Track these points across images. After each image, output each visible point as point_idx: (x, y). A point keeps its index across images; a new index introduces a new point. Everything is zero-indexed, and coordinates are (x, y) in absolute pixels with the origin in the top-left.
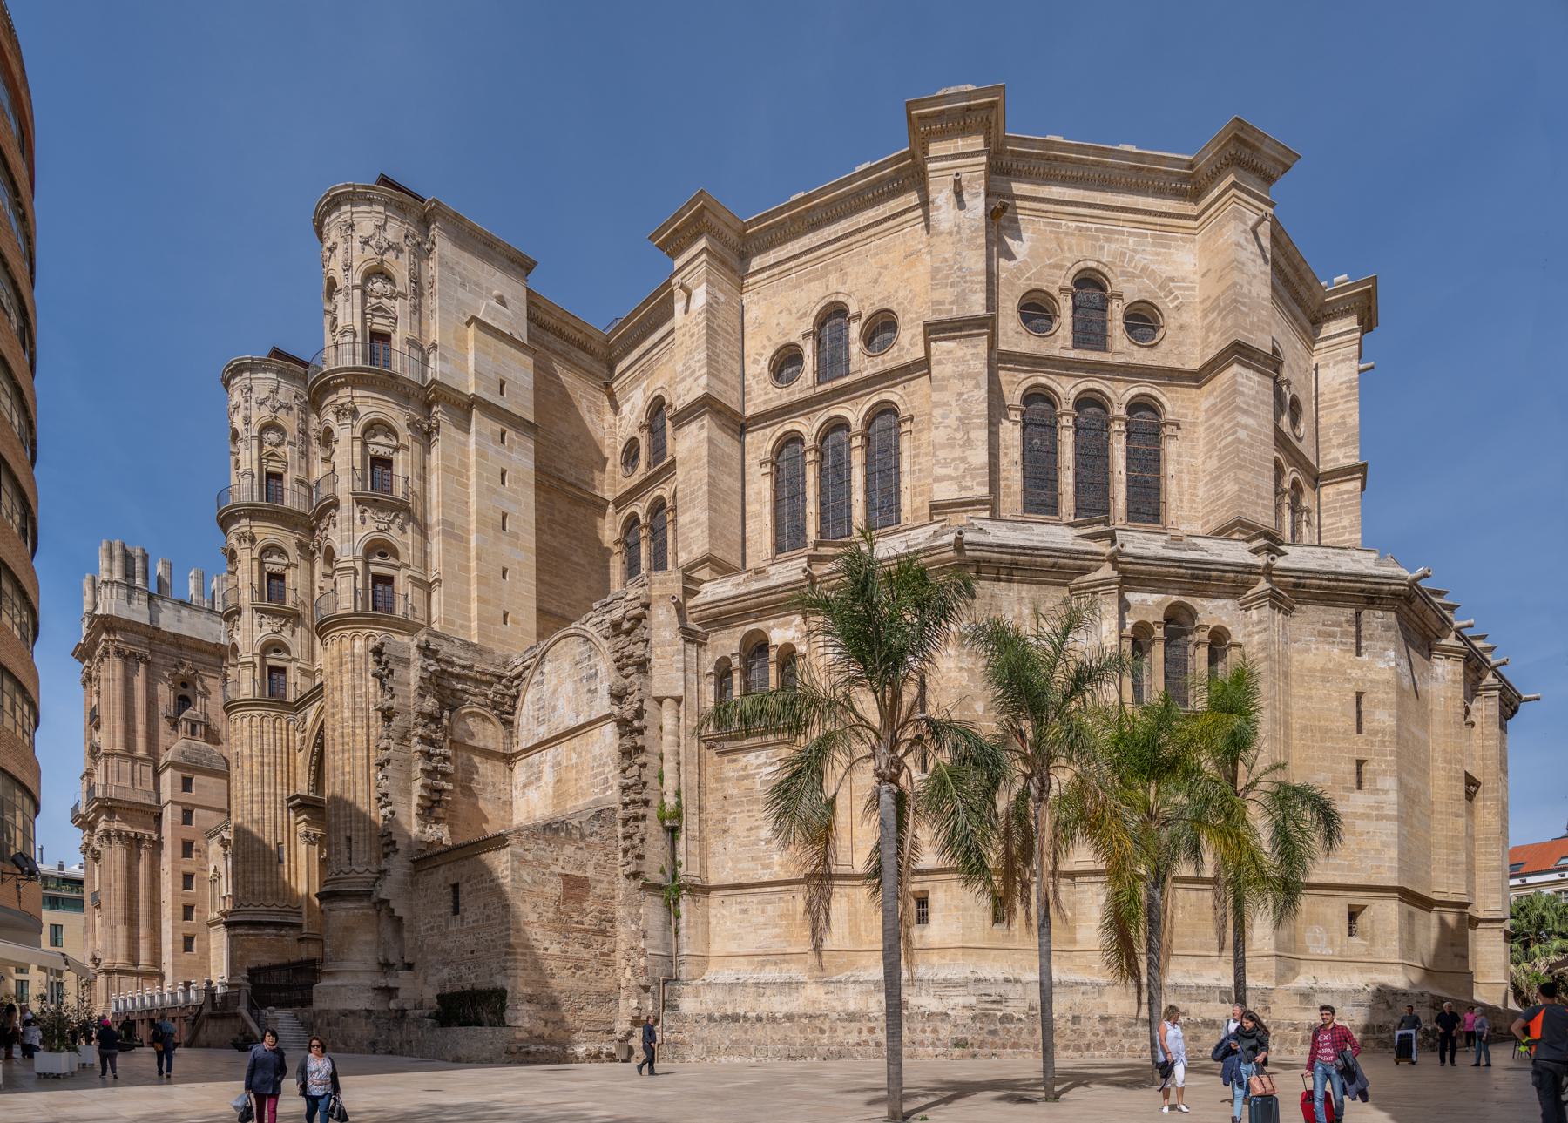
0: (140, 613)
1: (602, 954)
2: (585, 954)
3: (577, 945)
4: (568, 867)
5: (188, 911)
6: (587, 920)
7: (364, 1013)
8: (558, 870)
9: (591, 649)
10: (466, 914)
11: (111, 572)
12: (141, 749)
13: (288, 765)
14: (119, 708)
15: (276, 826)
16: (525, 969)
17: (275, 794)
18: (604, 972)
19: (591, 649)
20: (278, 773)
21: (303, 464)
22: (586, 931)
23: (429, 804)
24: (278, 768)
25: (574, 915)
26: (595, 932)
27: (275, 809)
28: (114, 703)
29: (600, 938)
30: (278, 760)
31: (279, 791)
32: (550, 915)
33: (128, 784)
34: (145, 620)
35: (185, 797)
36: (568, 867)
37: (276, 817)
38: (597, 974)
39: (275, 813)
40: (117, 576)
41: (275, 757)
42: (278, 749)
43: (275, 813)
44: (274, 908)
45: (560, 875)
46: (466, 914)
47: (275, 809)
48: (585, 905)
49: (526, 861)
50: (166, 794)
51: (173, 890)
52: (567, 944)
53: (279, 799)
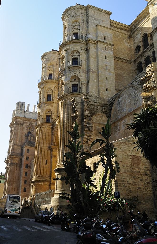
1: (148, 183)
2: (141, 183)
3: (139, 180)
4: (133, 152)
6: (141, 171)
8: (129, 154)
9: (135, 89)
10: (99, 172)
16: (121, 189)
18: (149, 189)
19: (135, 89)
22: (141, 175)
23: (87, 140)
25: (136, 169)
26: (144, 175)
29: (146, 177)
32: (129, 170)
36: (133, 152)
38: (146, 190)
45: (131, 156)
46: (99, 172)
48: (140, 166)
49: (120, 152)
52: (135, 179)
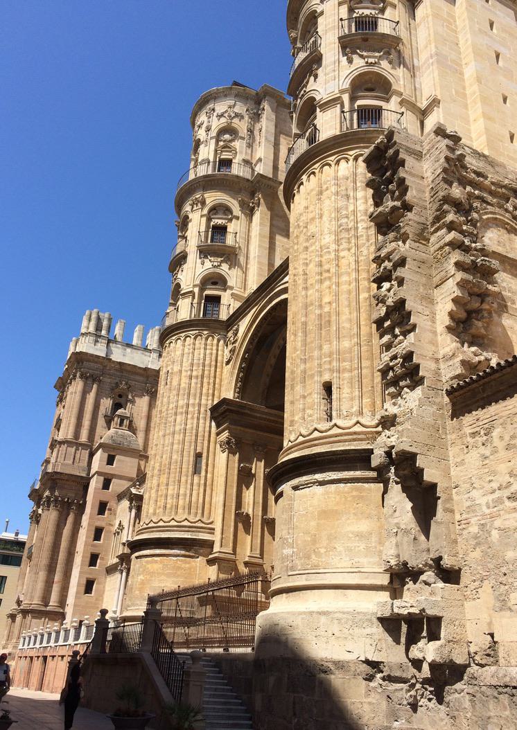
0: (100, 350)
5: (94, 559)
7: (365, 668)
11: (88, 328)
12: (84, 438)
13: (215, 377)
14: (75, 411)
15: (197, 436)
17: (200, 405)
20: (205, 384)
21: (249, 151)
24: (205, 380)
27: (198, 419)
28: (72, 408)
30: (206, 372)
31: (203, 402)
33: (71, 462)
34: (103, 355)
35: (109, 469)
37: (198, 426)
39: (198, 423)
40: (92, 329)
41: (203, 370)
42: (207, 362)
43: (198, 423)
44: (186, 523)
47: (198, 419)
50: (95, 467)
51: (86, 542)
53: (202, 409)
